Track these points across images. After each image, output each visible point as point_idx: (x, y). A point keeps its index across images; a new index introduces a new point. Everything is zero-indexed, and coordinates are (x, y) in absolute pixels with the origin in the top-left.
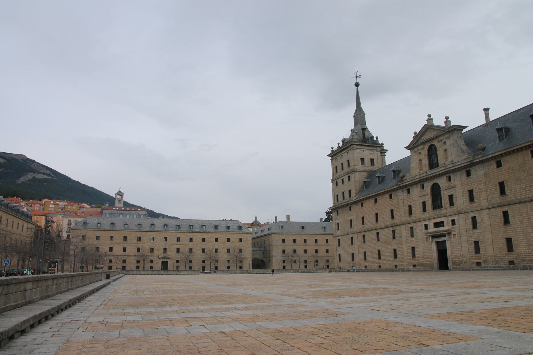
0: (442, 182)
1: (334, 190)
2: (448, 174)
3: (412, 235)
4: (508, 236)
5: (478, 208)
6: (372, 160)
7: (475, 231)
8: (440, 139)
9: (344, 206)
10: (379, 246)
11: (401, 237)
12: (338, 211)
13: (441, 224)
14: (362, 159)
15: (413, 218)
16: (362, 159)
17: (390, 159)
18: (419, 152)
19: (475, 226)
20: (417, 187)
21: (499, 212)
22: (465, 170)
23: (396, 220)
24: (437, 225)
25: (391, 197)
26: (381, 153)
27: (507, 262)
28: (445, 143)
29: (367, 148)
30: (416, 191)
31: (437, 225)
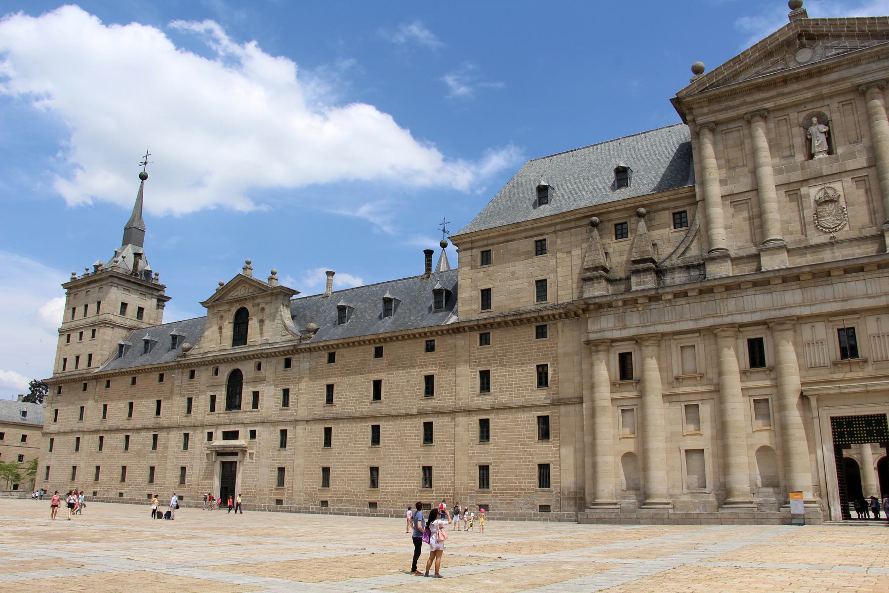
0: (247, 370)
1: (59, 349)
2: (259, 359)
3: (186, 446)
4: (326, 465)
5: (292, 418)
6: (141, 310)
7: (283, 452)
8: (257, 301)
9: (74, 381)
10: (124, 459)
11: (166, 448)
12: (60, 388)
13: (234, 435)
14: (124, 305)
15: (192, 419)
16: (124, 305)
17: (170, 315)
18: (221, 314)
19: (283, 444)
20: (207, 370)
21: (320, 429)
22: (284, 357)
23: (164, 419)
24: (228, 435)
25: (161, 378)
26: (159, 300)
27: (318, 502)
28: (263, 309)
29: (136, 287)
30: (204, 376)
31: (228, 435)
